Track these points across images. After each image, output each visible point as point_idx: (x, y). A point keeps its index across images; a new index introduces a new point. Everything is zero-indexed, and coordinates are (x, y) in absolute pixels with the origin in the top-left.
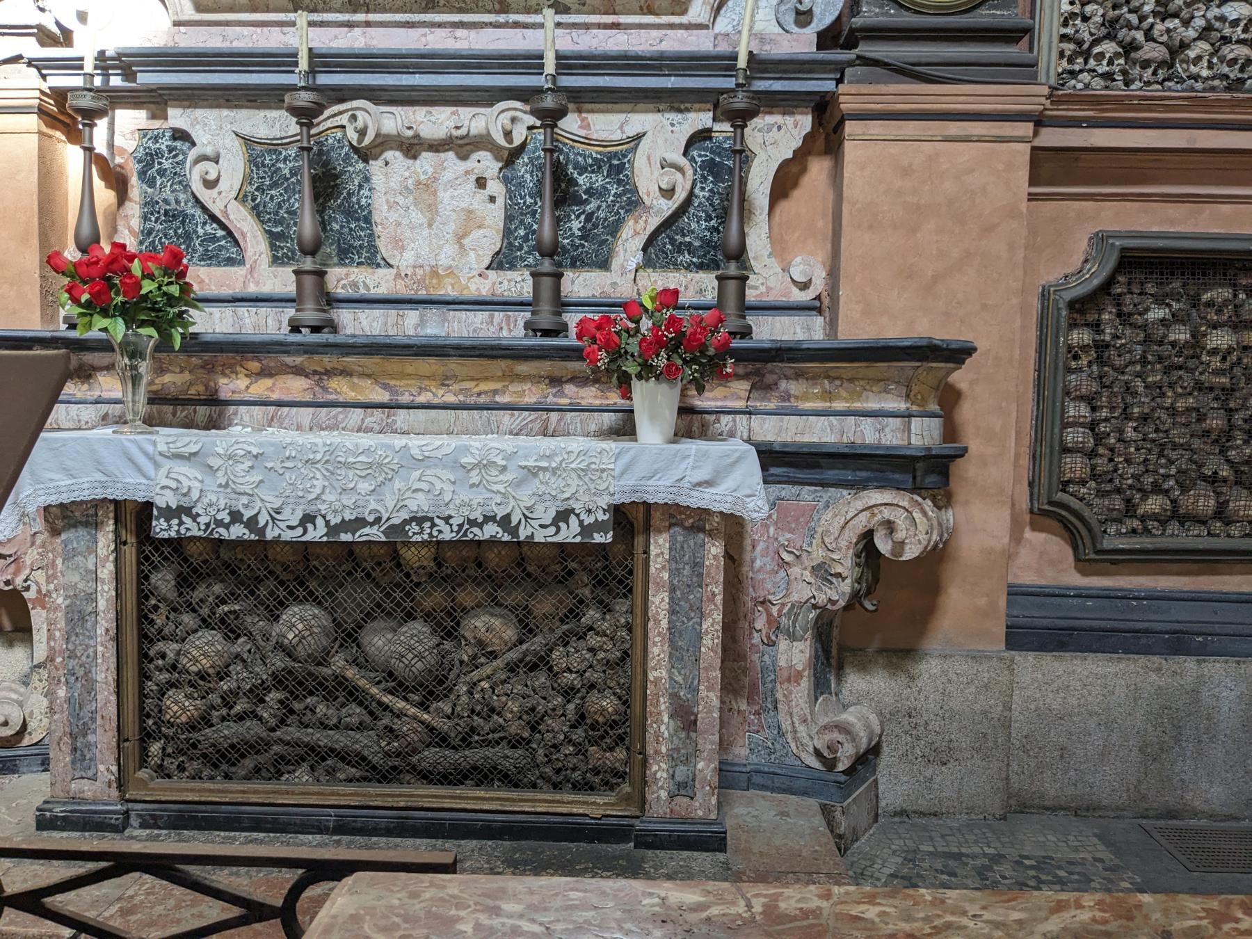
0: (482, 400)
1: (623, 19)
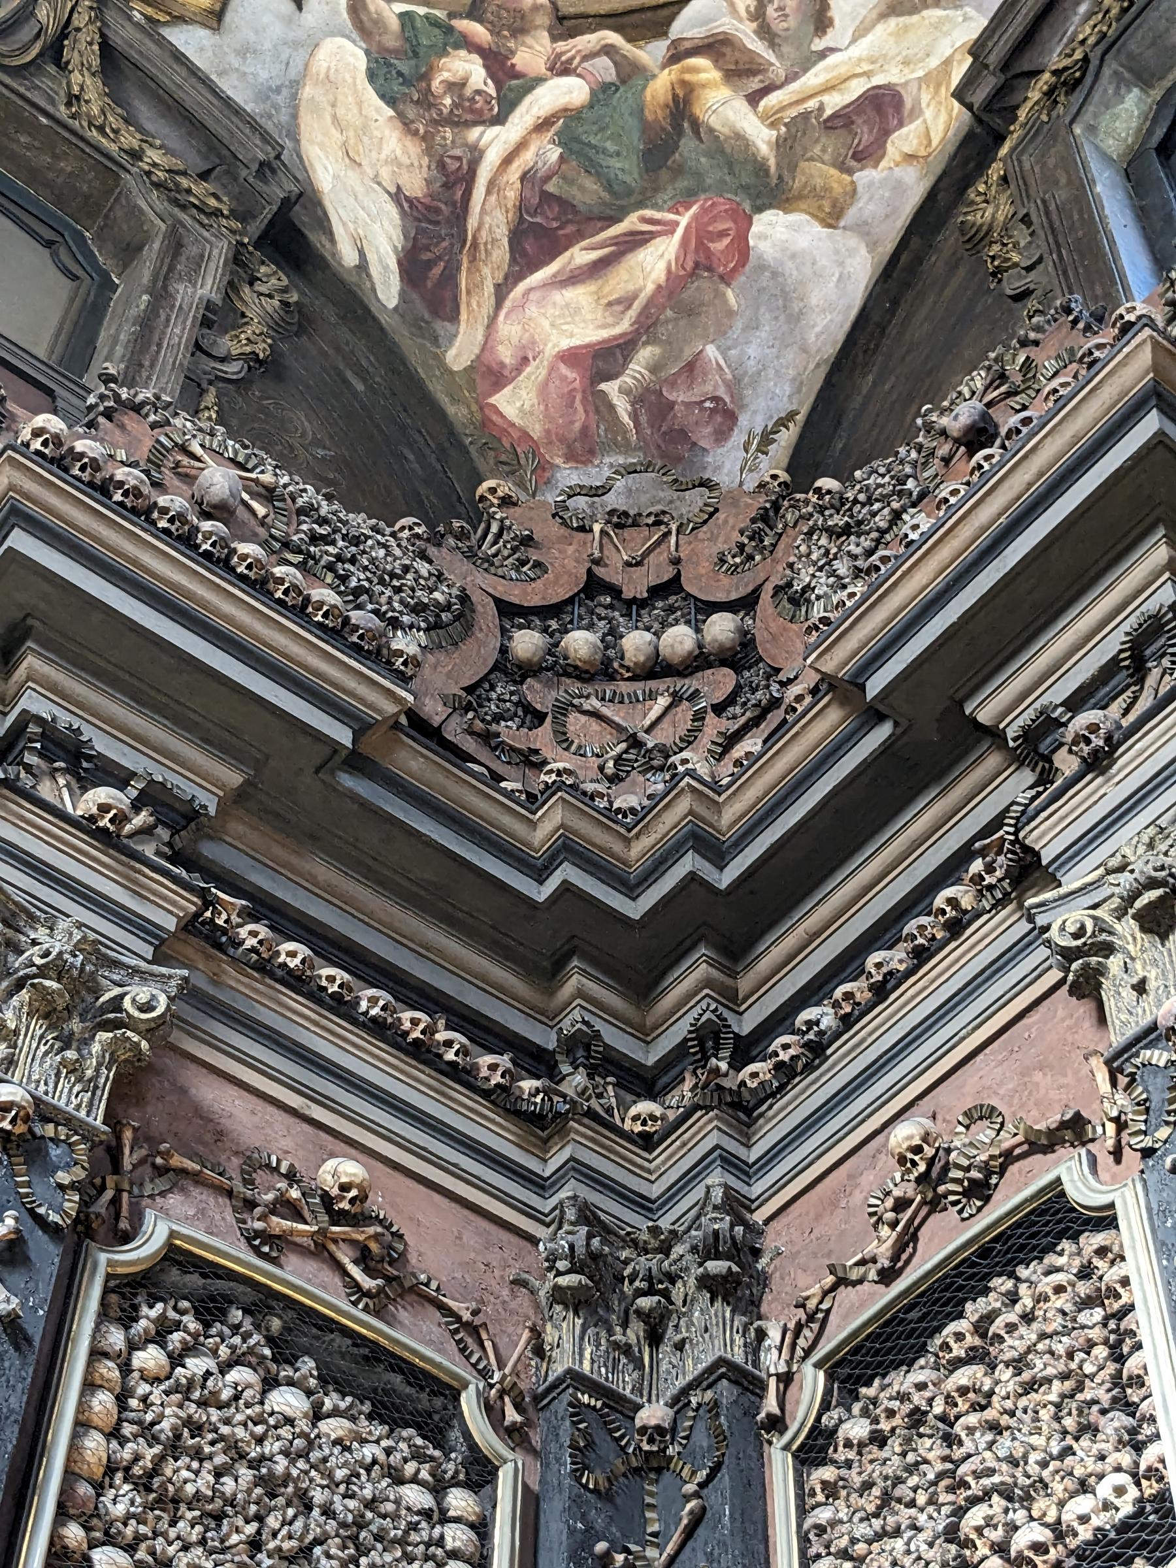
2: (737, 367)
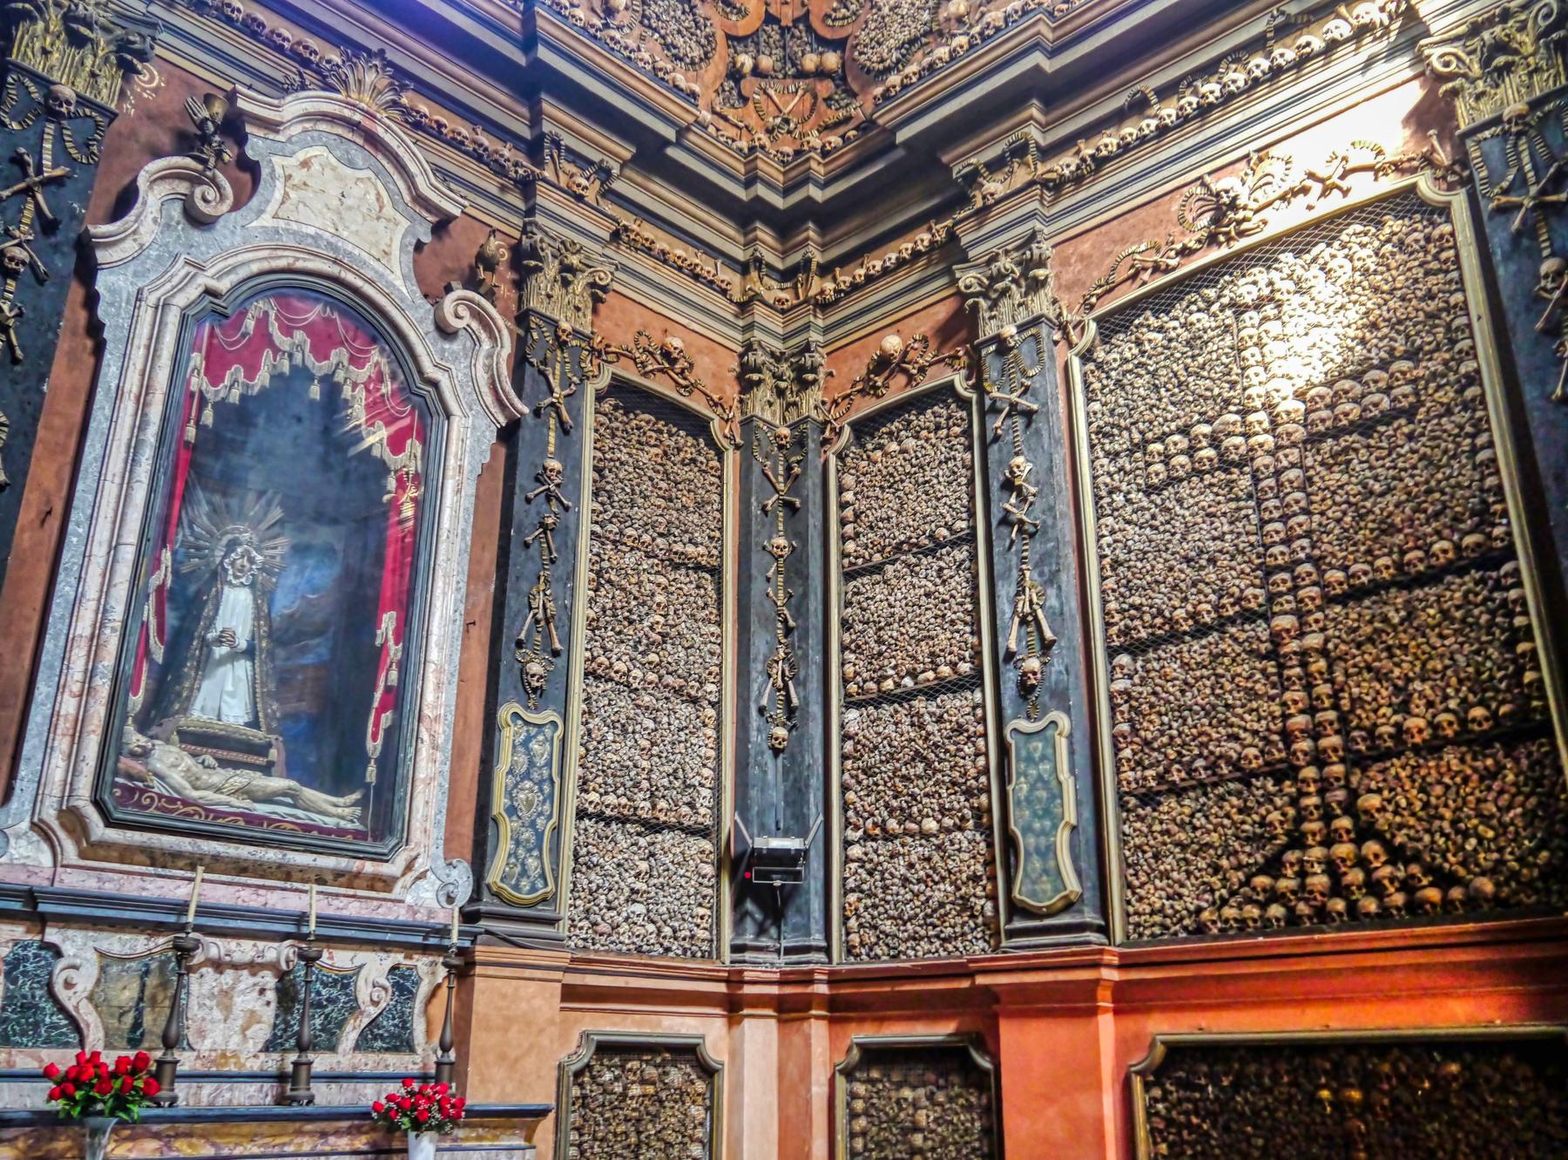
0: (276, 1150)
1: (360, 893)
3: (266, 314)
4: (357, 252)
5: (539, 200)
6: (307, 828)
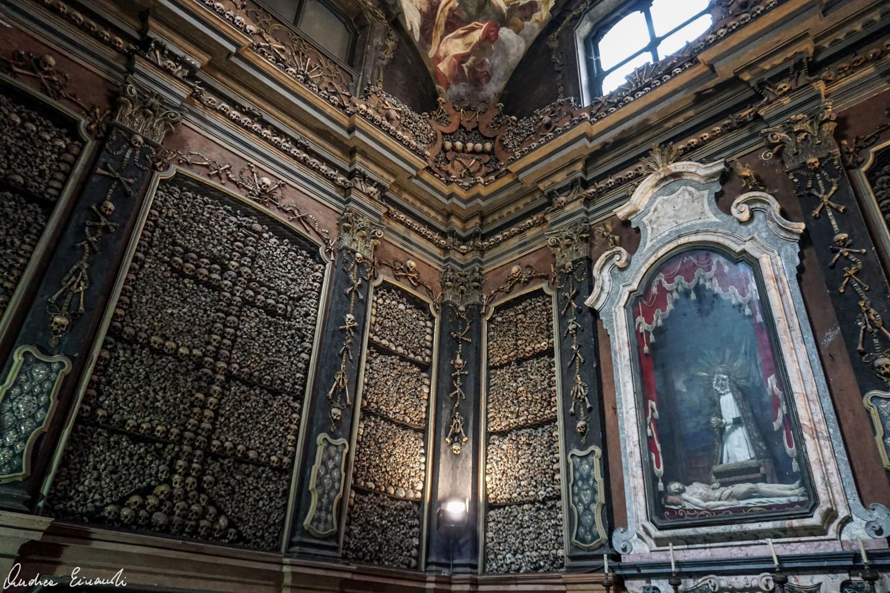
1: (802, 539)
2: (493, 65)
3: (660, 281)
4: (689, 224)
5: (765, 118)
6: (769, 508)
